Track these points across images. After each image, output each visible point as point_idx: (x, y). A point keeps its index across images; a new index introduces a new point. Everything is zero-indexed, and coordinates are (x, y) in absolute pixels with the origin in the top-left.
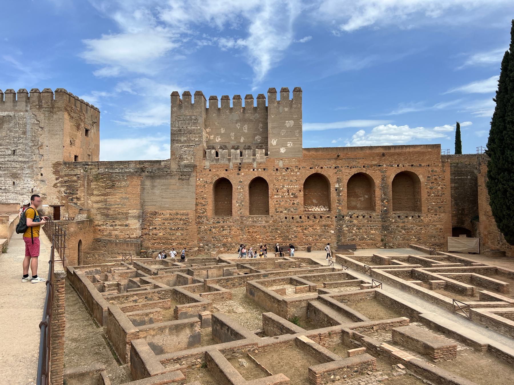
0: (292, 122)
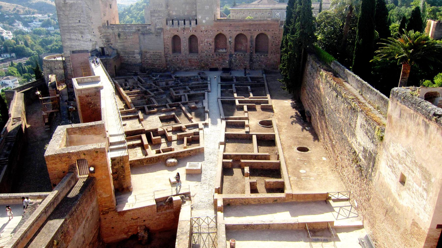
0: (208, 7)
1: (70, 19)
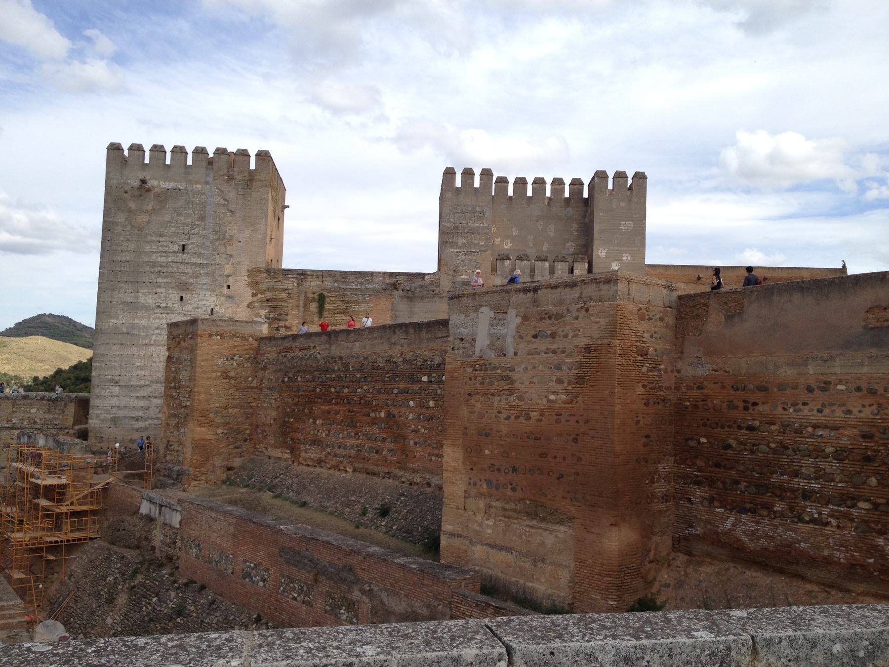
0: (630, 224)
1: (149, 238)
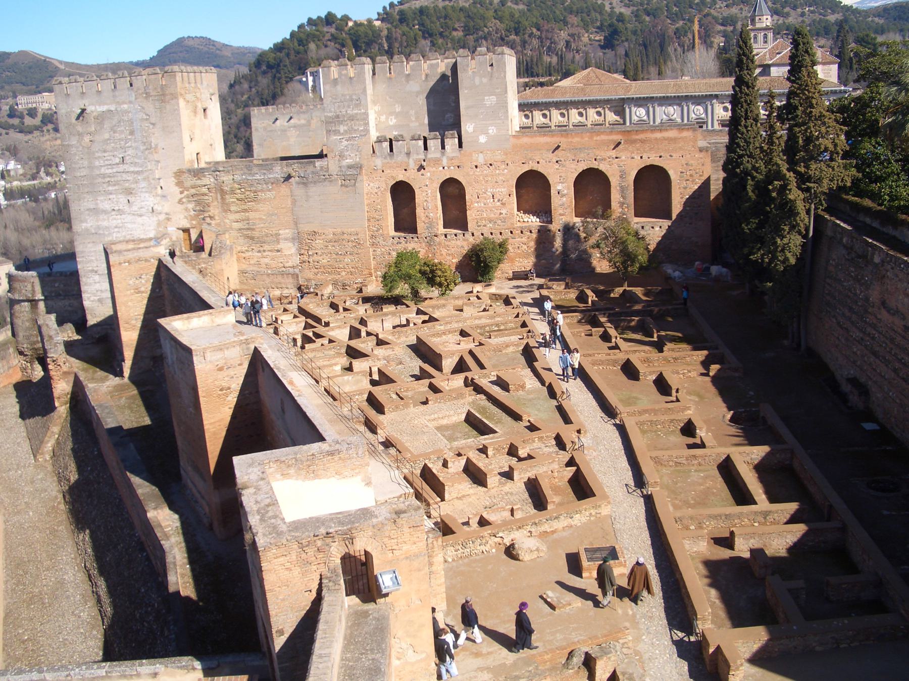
1: (97, 155)
